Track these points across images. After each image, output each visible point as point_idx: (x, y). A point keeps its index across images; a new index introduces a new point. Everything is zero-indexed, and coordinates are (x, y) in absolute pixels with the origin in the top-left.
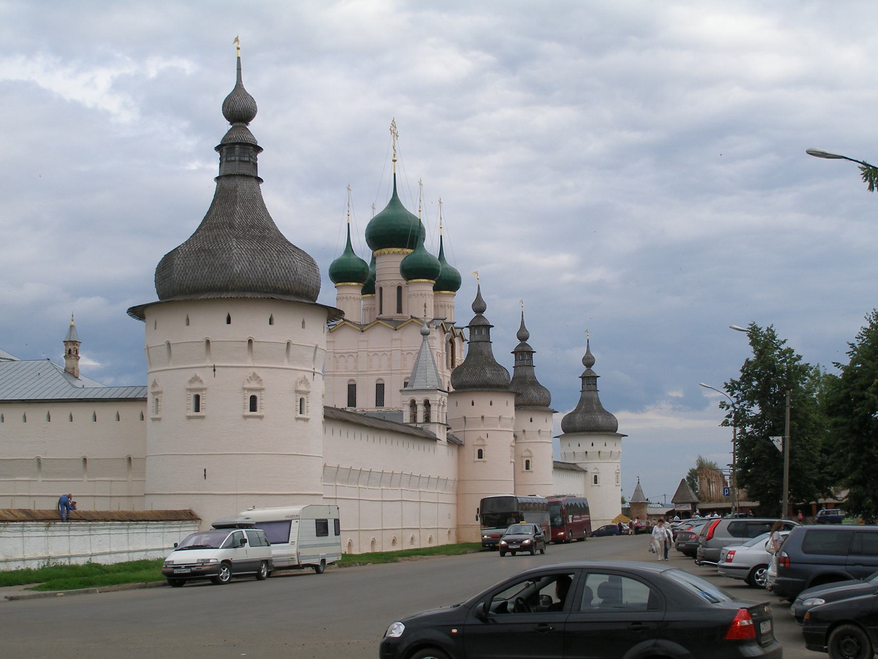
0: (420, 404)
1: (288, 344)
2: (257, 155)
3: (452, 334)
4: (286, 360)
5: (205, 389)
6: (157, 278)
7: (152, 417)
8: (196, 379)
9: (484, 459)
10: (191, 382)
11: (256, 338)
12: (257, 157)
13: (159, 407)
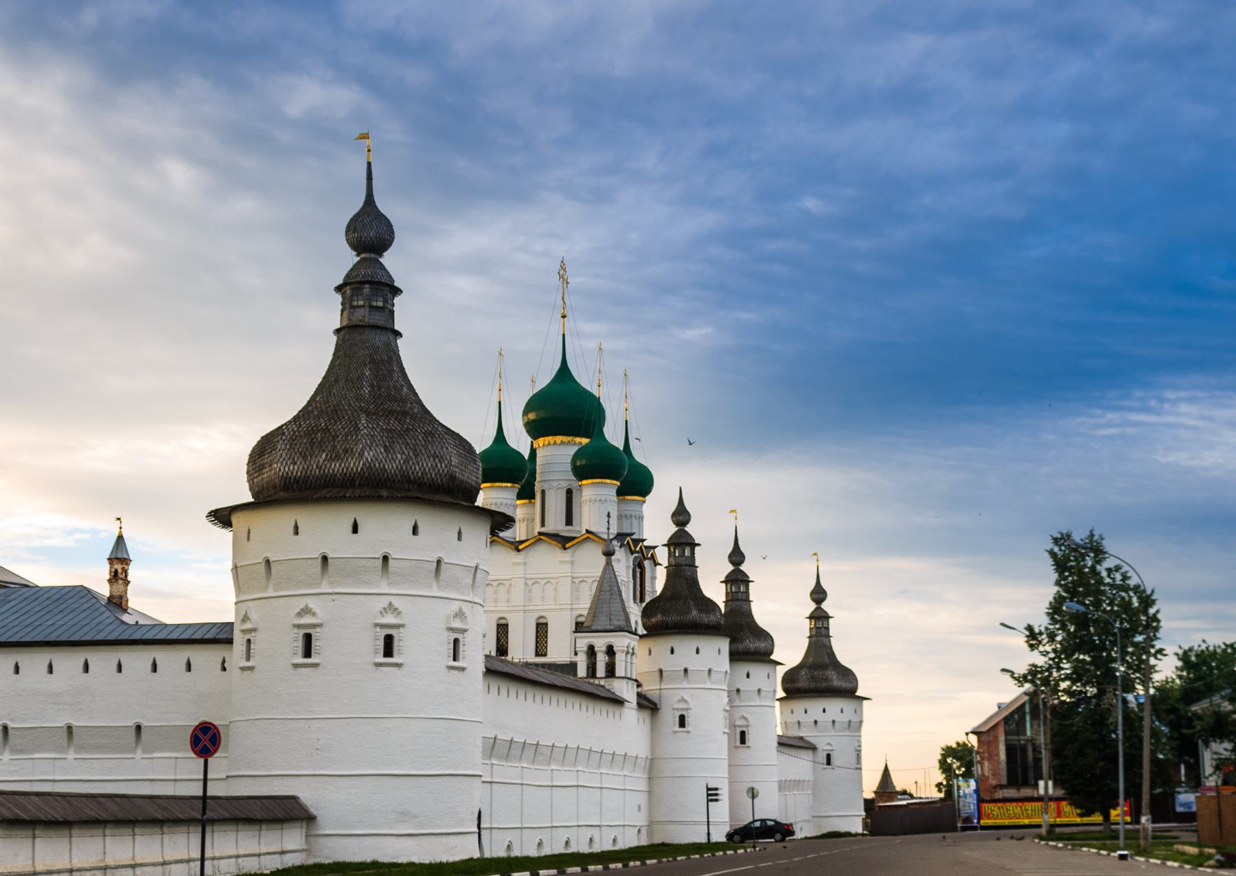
1: (439, 562)
2: (393, 299)
3: (640, 555)
4: (435, 583)
6: (251, 468)
8: (306, 611)
10: (299, 614)
11: (393, 554)
12: (394, 302)
13: (252, 651)
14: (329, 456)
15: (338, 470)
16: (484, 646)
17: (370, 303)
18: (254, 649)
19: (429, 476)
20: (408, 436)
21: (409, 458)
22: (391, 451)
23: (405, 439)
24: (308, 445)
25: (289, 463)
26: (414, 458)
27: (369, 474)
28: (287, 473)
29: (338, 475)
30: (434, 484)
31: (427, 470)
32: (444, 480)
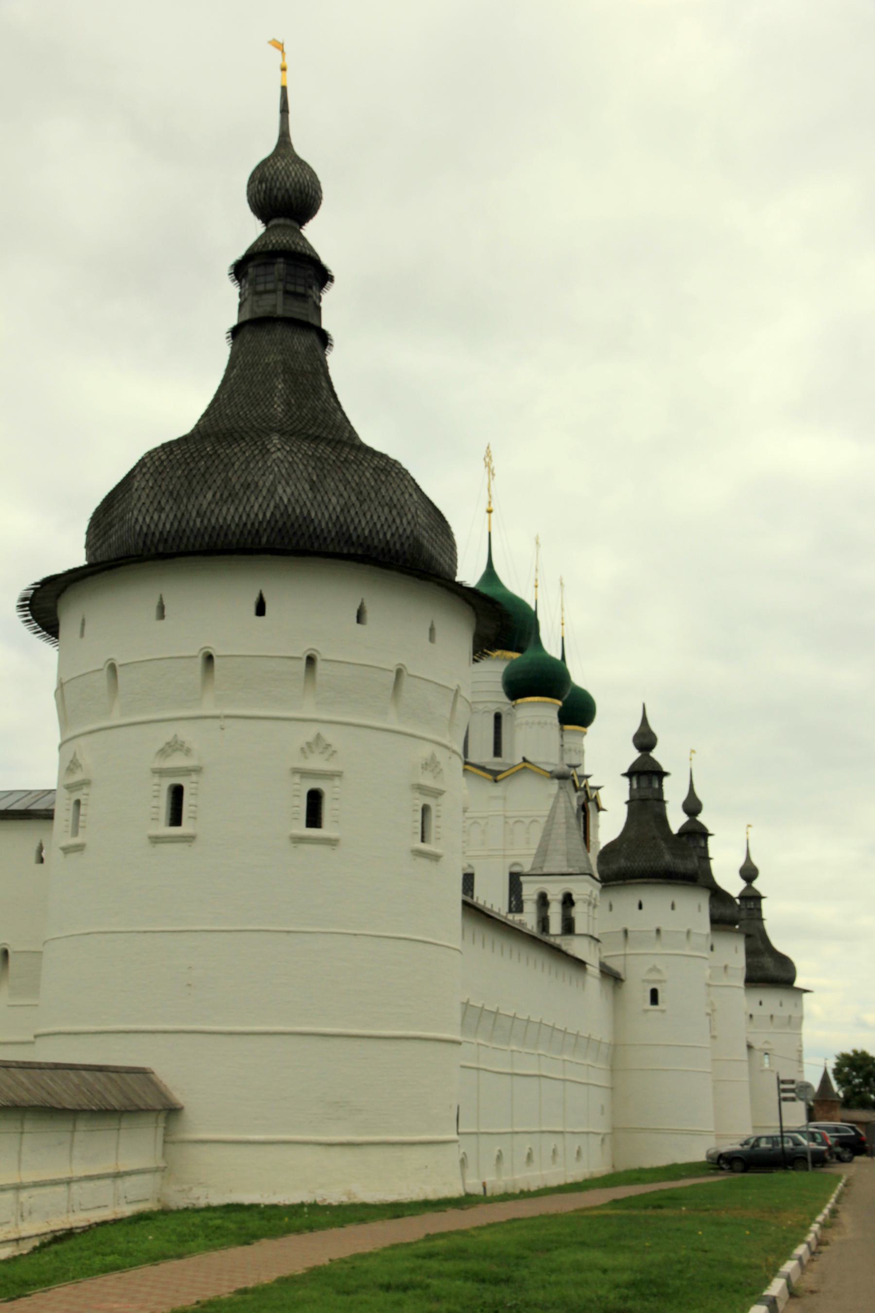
0: (555, 900)
1: (399, 673)
5: (198, 770)
7: (64, 844)
8: (174, 746)
9: (661, 1005)
10: (163, 752)
11: (323, 653)
13: (81, 818)
14: (218, 495)
15: (233, 517)
16: (464, 827)
17: (285, 287)
18: (85, 815)
19: (381, 536)
20: (347, 469)
21: (350, 504)
22: (321, 489)
23: (344, 475)
24: (183, 479)
25: (151, 510)
26: (357, 504)
27: (284, 523)
28: (149, 526)
29: (233, 527)
30: (390, 550)
31: (379, 526)
32: (406, 546)
